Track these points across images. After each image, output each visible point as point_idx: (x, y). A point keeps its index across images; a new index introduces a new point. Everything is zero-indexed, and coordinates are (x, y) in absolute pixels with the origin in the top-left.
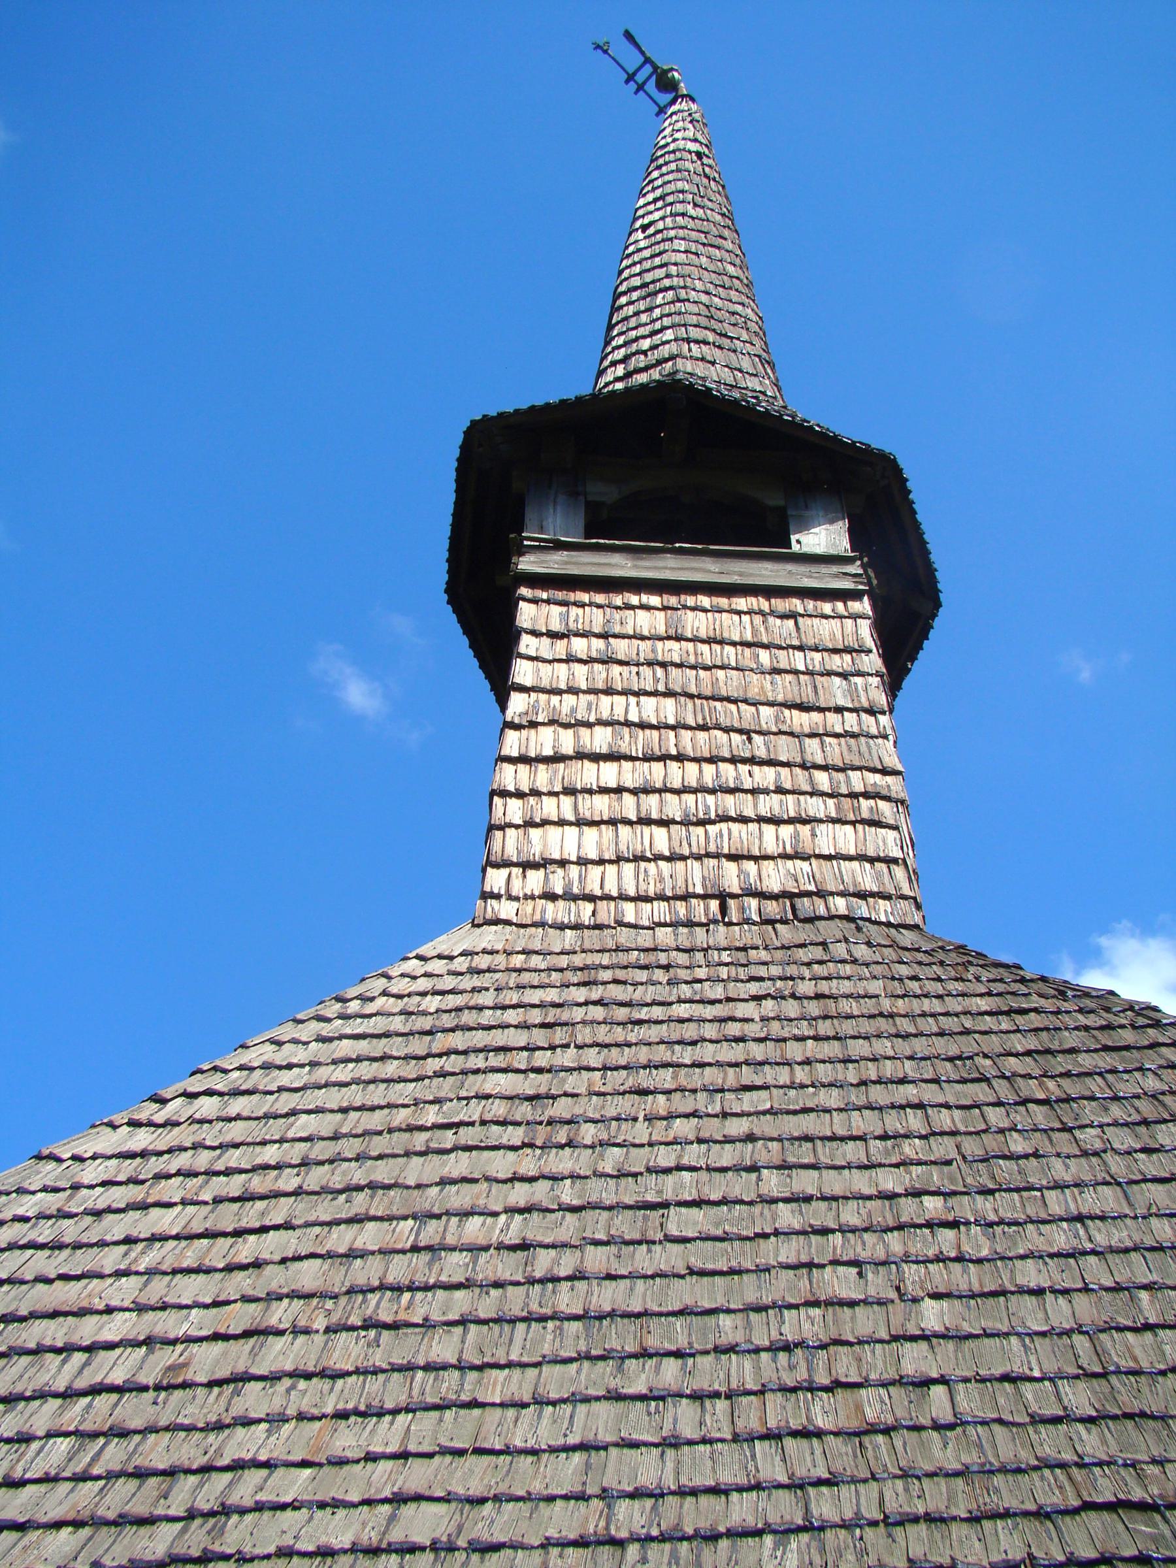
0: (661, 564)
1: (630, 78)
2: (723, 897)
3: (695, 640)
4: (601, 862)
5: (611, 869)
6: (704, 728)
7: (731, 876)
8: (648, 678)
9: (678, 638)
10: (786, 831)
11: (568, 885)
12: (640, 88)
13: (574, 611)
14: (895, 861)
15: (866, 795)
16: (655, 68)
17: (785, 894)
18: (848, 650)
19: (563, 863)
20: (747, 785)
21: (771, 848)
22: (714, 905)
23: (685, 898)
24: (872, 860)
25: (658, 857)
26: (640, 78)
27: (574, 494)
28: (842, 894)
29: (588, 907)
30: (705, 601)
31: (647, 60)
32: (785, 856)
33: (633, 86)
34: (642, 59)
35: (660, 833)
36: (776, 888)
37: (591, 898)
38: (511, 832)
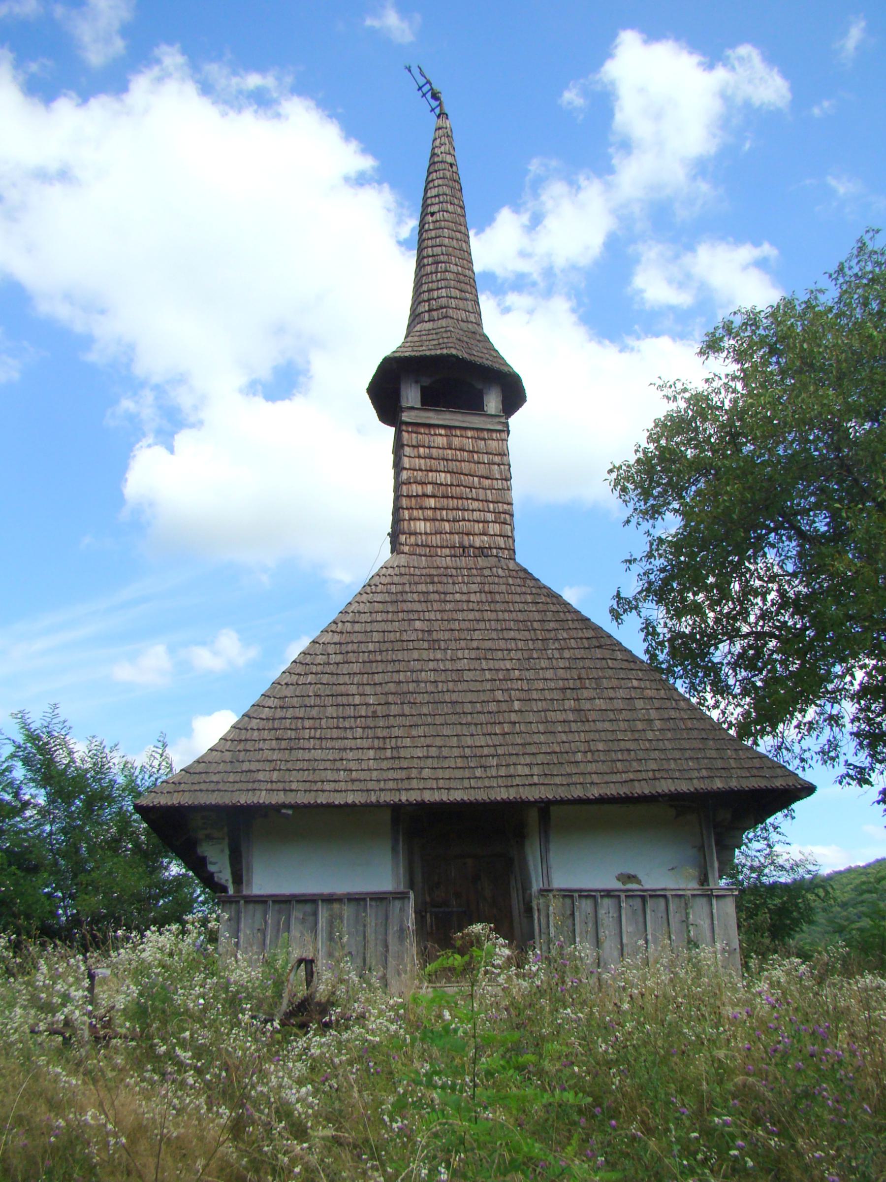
0: (445, 417)
1: (420, 89)
2: (464, 548)
3: (455, 449)
4: (431, 534)
5: (434, 537)
6: (458, 486)
7: (466, 541)
8: (442, 465)
9: (451, 449)
10: (481, 525)
11: (422, 542)
12: (424, 95)
13: (420, 436)
14: (508, 537)
15: (503, 513)
16: (432, 89)
17: (480, 548)
18: (500, 454)
19: (421, 534)
20: (471, 508)
21: (477, 531)
22: (461, 550)
23: (454, 547)
24: (504, 536)
25: (446, 533)
27: (417, 382)
28: (495, 548)
29: (428, 550)
30: (458, 433)
31: (428, 82)
32: (480, 534)
33: (420, 93)
34: (425, 81)
35: (447, 524)
36: (478, 546)
37: (429, 546)
38: (406, 523)
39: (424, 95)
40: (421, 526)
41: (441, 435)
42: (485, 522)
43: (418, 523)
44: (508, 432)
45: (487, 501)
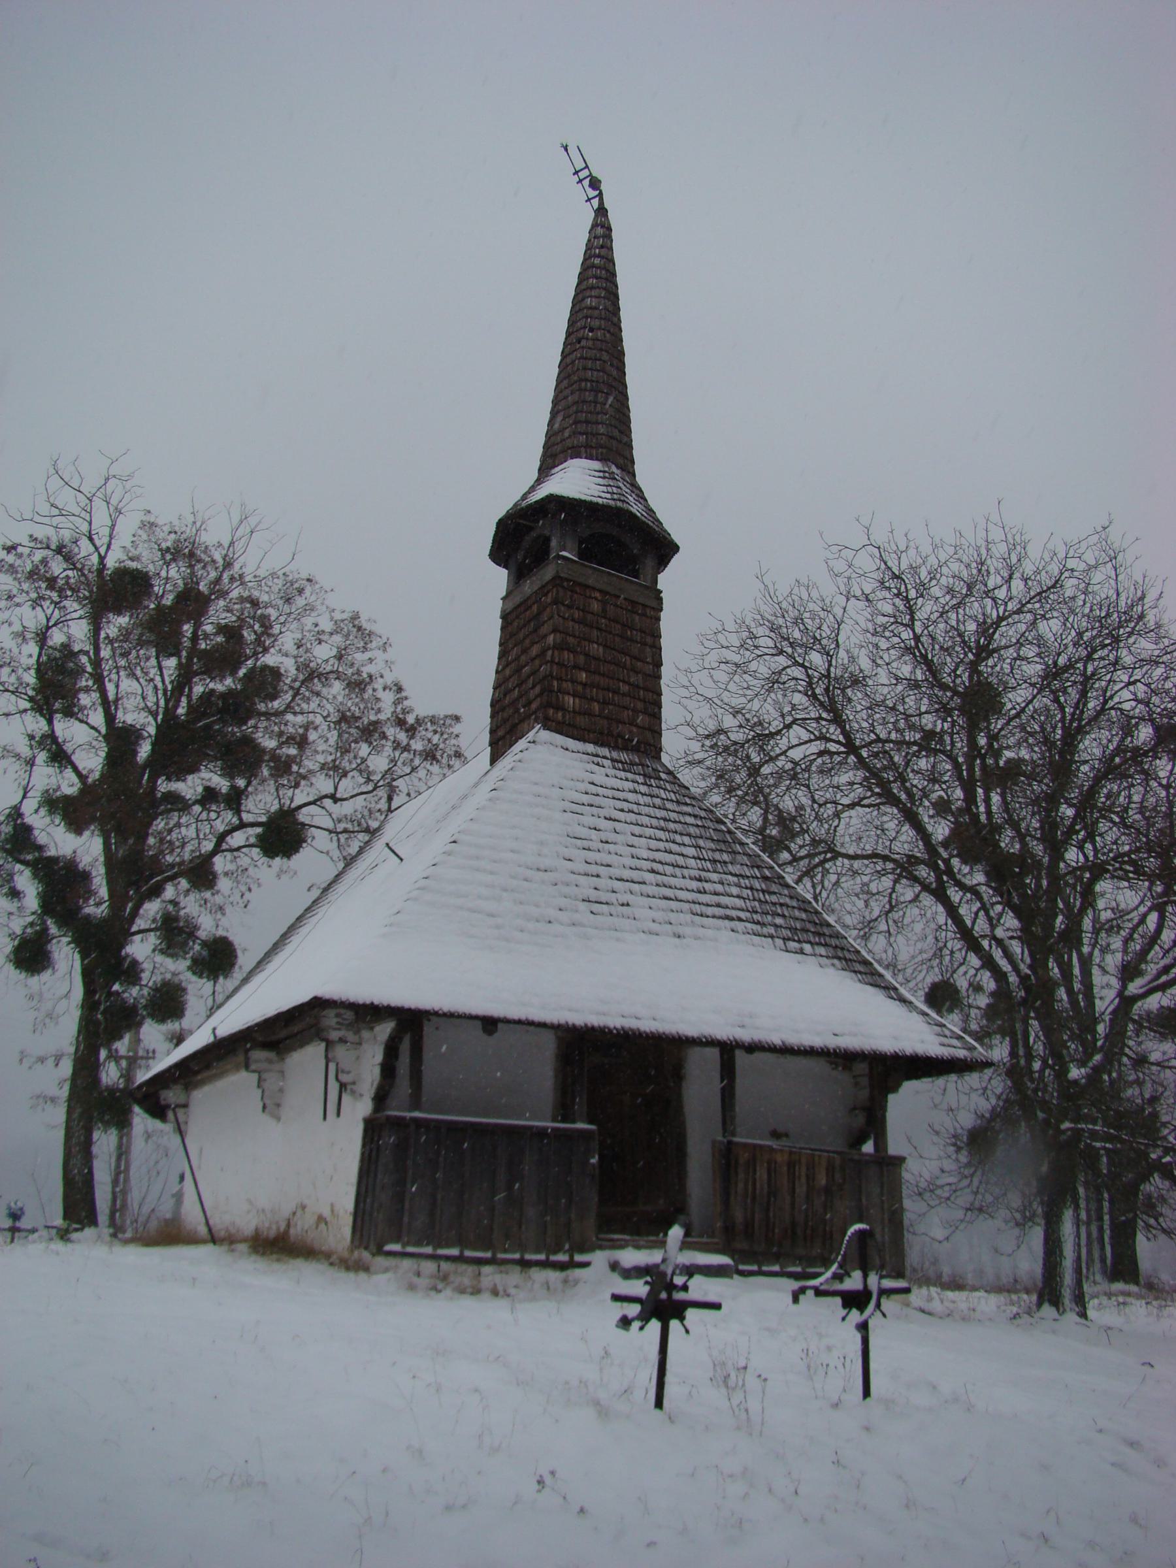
1: (576, 173)
9: (605, 618)
12: (580, 181)
16: (591, 174)
26: (582, 175)
31: (587, 167)
39: (580, 181)
40: (570, 701)
41: (596, 599)
42: (634, 710)
43: (566, 698)
44: (661, 610)
45: (638, 686)
